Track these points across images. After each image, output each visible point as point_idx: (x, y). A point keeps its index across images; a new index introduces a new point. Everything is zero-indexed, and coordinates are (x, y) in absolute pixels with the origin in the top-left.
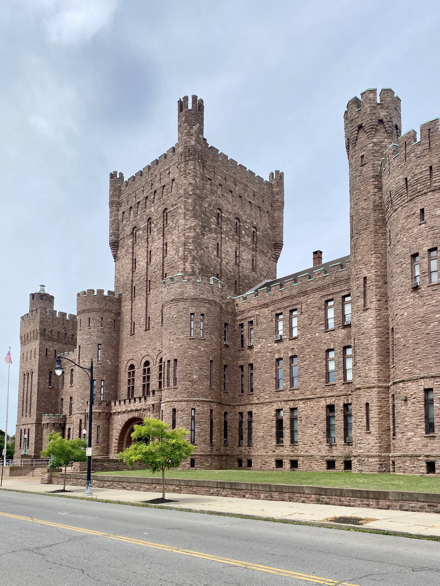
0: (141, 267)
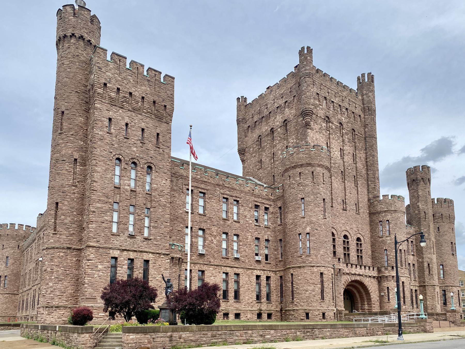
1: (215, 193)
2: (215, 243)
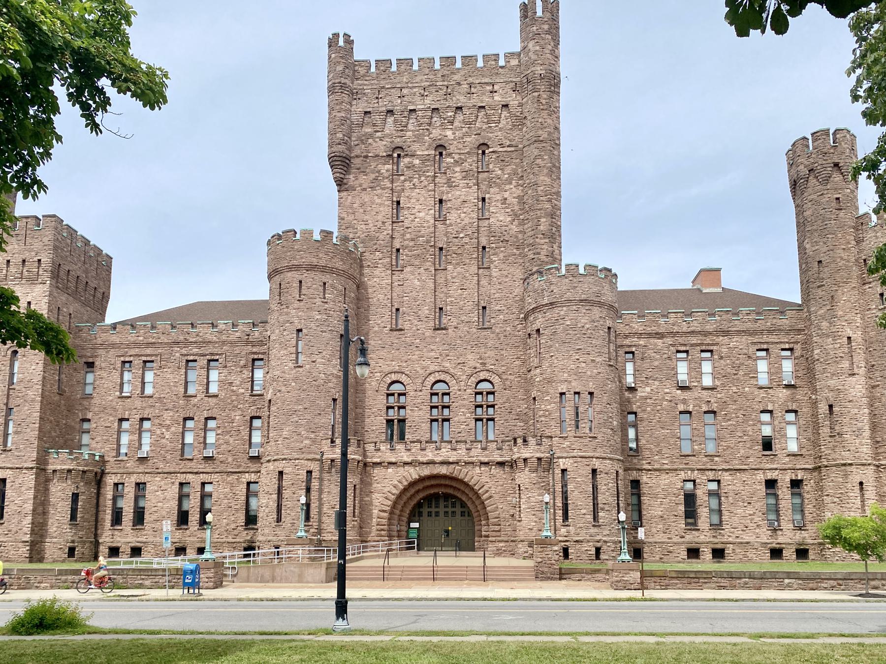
0: (416, 220)
1: (172, 357)
2: (167, 437)
